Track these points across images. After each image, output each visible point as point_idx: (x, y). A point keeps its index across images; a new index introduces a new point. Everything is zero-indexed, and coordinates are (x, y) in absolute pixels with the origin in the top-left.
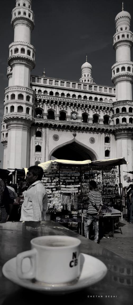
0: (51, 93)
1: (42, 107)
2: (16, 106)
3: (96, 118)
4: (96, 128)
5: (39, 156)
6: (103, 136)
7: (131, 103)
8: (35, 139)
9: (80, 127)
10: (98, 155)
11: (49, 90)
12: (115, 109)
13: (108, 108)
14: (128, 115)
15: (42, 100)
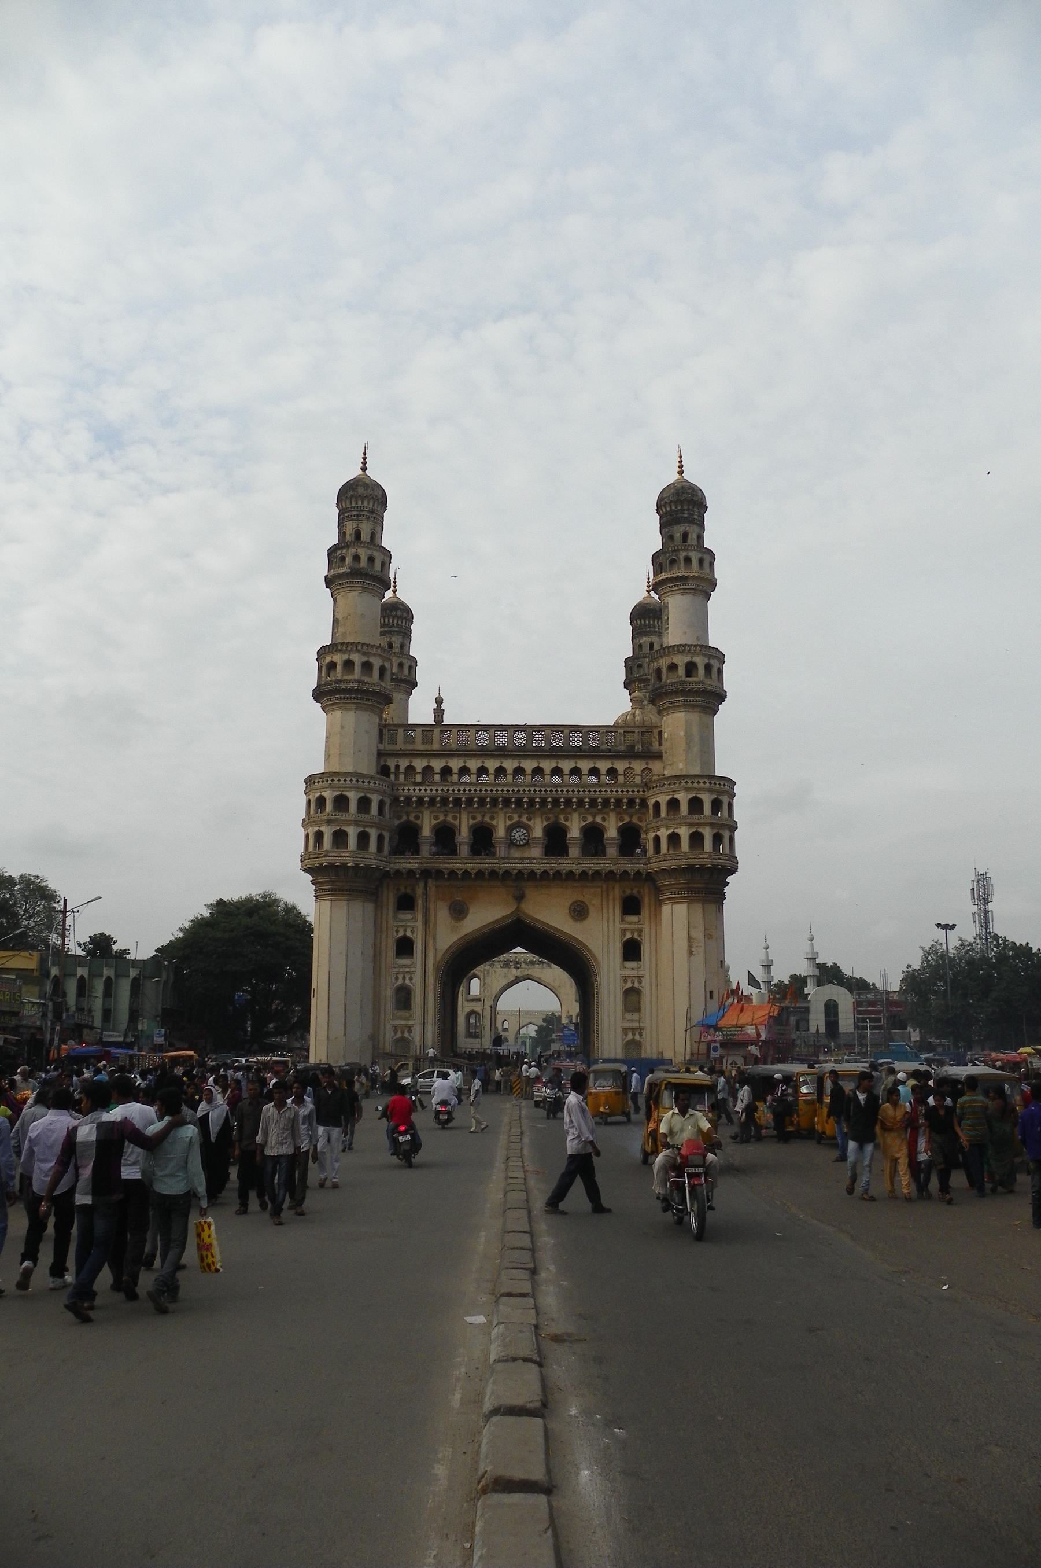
0: (446, 771)
1: (417, 818)
2: (328, 831)
3: (593, 836)
4: (587, 869)
5: (407, 970)
6: (617, 892)
7: (696, 784)
8: (395, 918)
9: (532, 874)
10: (600, 958)
11: (437, 764)
12: (651, 802)
13: (631, 802)
14: (686, 824)
15: (414, 799)
